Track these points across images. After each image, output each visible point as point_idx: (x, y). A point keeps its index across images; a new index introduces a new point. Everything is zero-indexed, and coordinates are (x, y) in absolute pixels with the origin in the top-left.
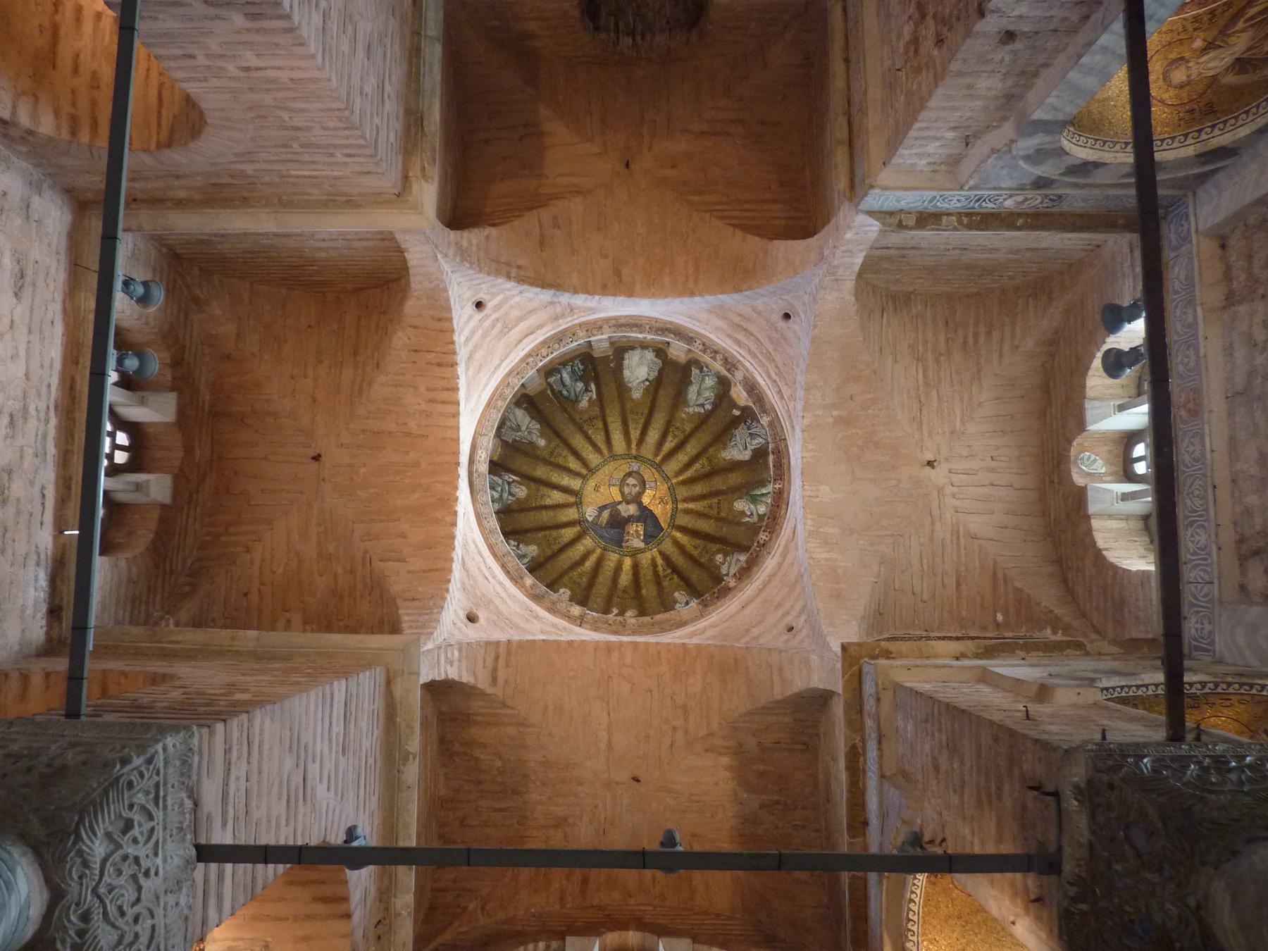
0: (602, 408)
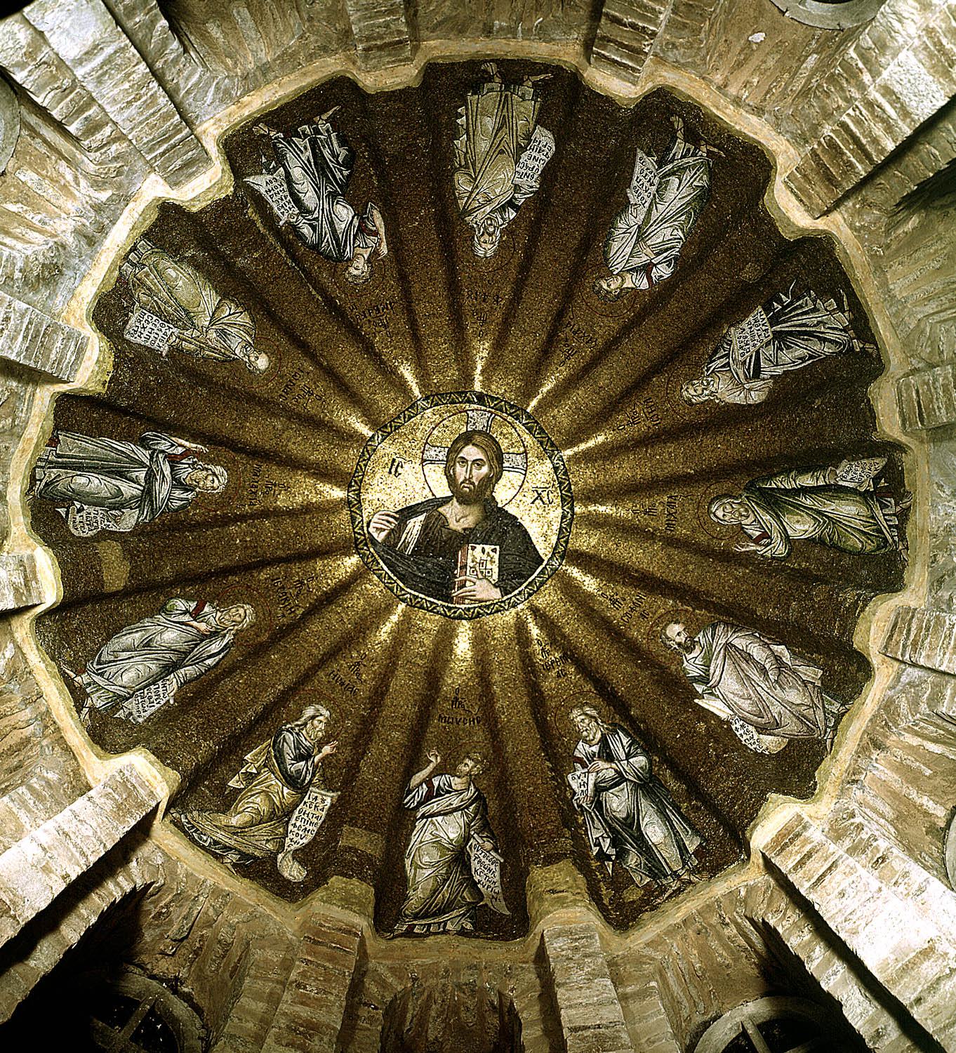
0: (403, 278)
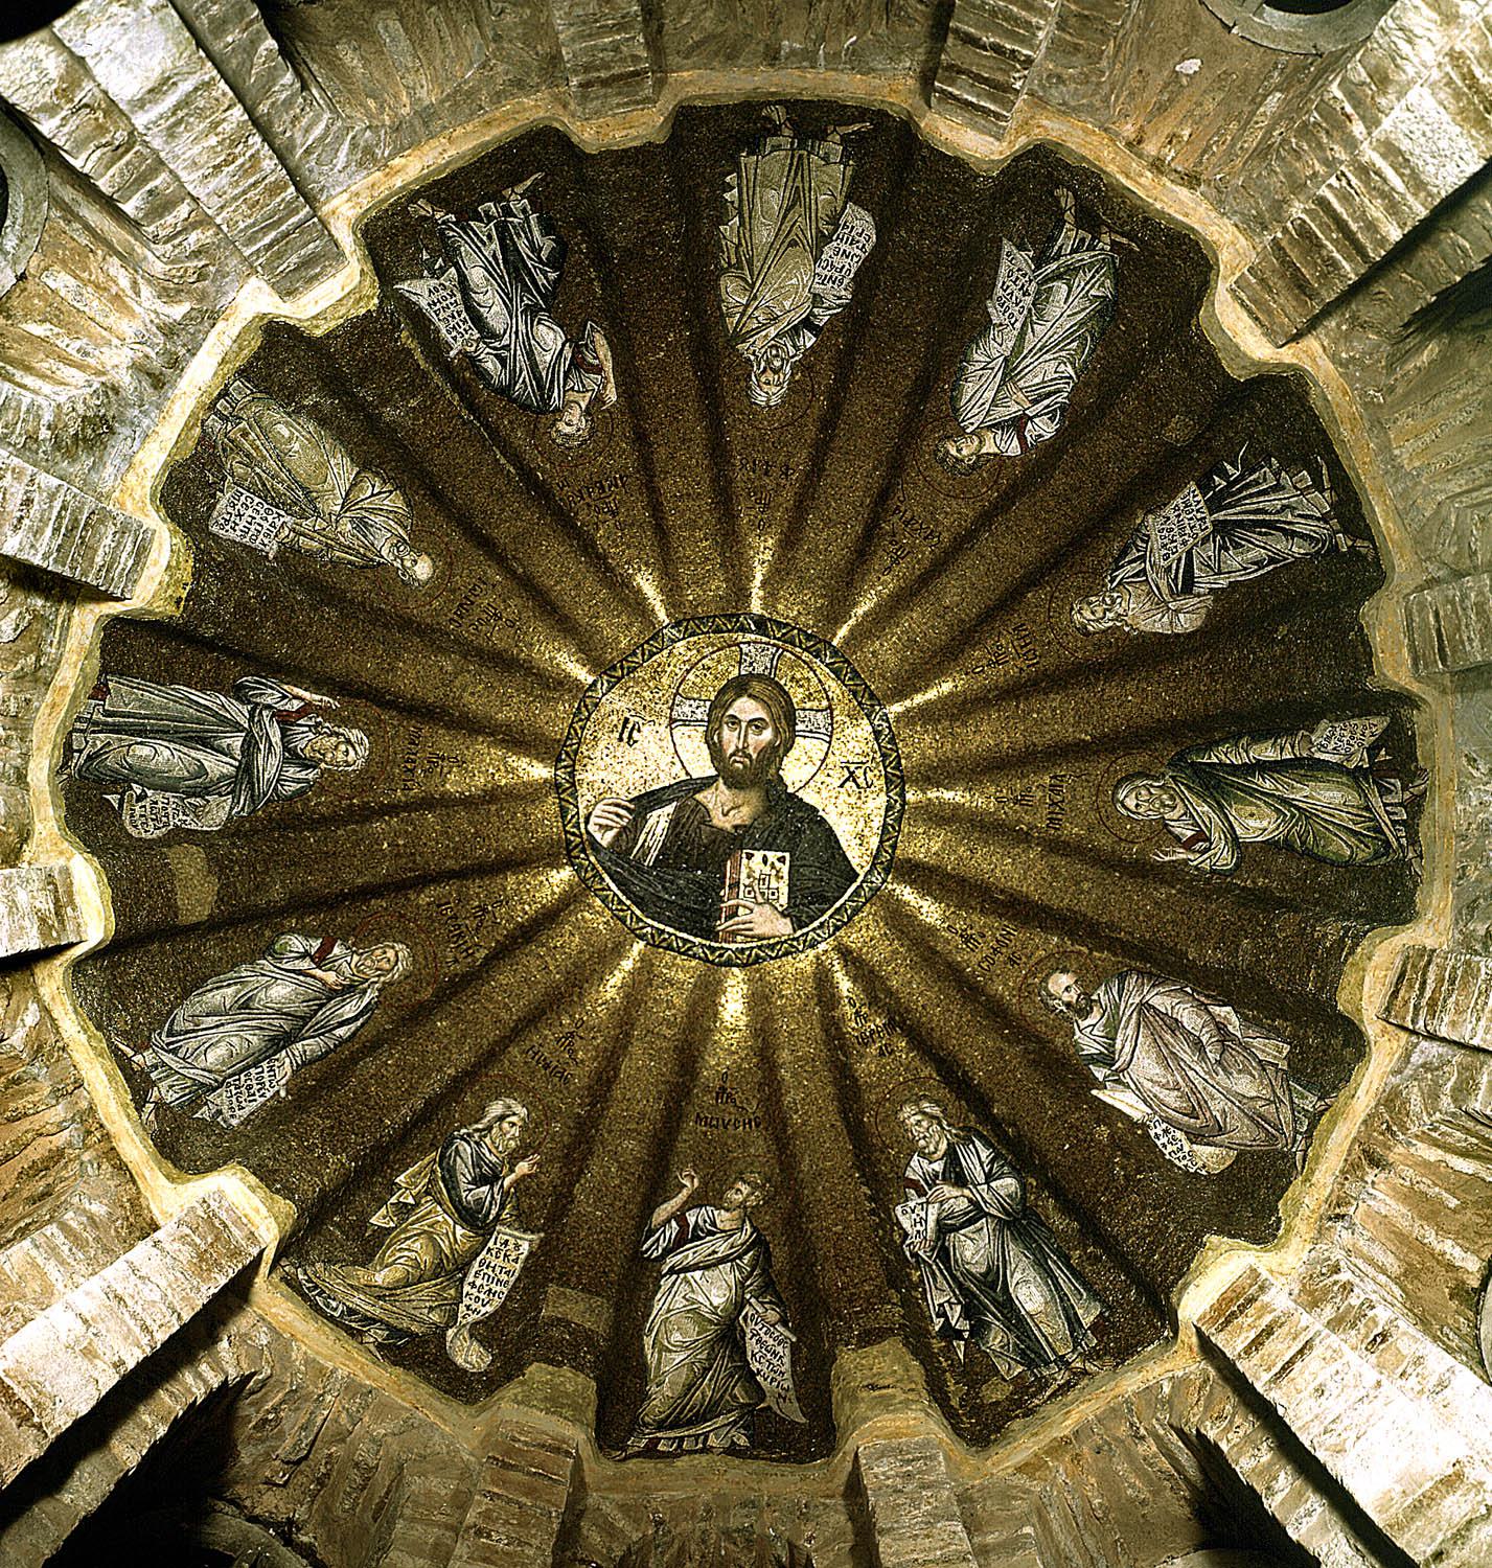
0: (641, 438)
